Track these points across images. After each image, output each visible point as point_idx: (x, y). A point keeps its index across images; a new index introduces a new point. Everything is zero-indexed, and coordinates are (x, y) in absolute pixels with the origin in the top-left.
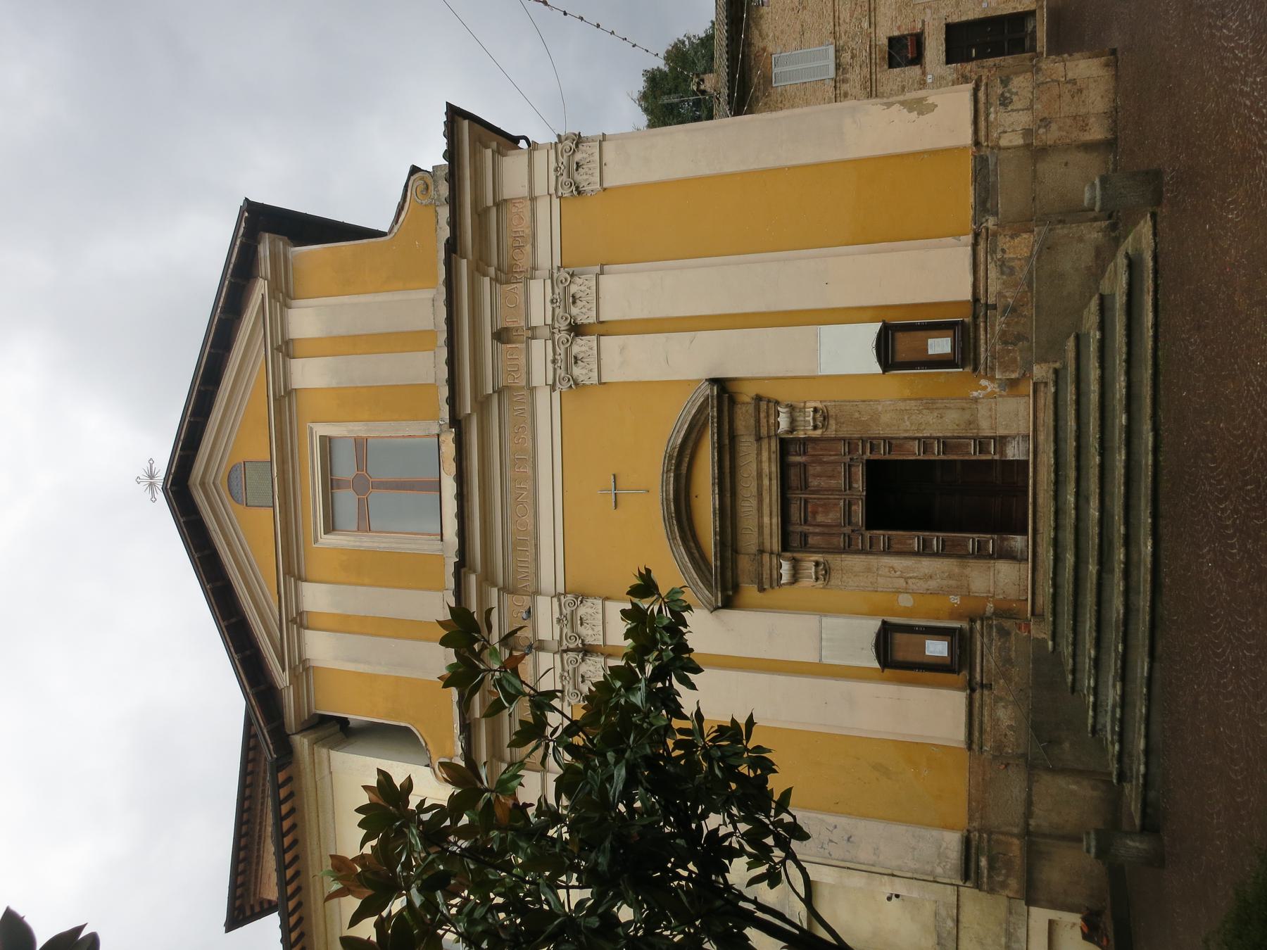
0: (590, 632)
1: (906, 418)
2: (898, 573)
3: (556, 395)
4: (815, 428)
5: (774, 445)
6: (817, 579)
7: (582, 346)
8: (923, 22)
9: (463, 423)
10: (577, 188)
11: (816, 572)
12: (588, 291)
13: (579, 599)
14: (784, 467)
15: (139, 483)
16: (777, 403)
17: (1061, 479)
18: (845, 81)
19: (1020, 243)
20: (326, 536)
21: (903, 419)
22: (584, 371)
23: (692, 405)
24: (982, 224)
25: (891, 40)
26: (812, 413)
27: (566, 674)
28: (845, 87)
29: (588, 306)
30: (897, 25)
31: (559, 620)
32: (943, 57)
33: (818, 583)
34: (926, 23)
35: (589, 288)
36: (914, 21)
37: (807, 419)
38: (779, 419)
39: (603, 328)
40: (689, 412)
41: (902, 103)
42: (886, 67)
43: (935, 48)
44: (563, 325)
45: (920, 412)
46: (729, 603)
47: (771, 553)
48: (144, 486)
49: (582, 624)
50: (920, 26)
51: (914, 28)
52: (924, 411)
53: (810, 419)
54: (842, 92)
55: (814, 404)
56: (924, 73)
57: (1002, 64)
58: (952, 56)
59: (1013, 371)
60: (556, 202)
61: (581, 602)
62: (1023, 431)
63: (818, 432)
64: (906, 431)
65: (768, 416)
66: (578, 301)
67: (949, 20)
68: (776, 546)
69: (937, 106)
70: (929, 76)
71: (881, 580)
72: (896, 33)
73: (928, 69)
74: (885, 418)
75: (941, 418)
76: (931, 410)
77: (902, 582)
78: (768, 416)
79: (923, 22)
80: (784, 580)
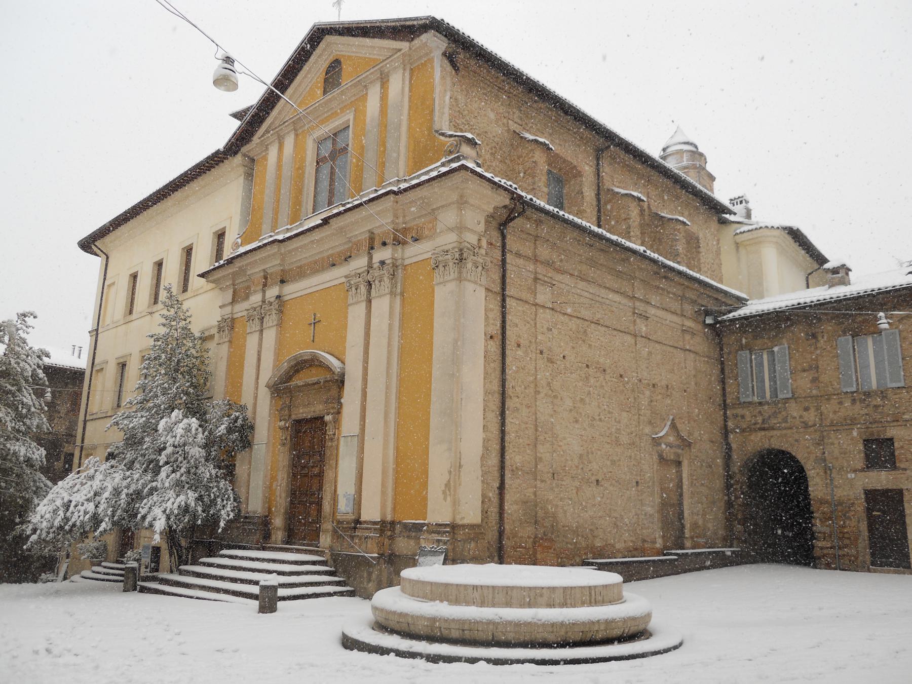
7: (363, 289)
8: (906, 470)
18: (854, 401)
25: (891, 440)
28: (847, 404)
30: (905, 445)
32: (870, 487)
34: (904, 472)
36: (907, 461)
42: (864, 437)
43: (881, 479)
50: (902, 466)
51: (900, 461)
54: (843, 400)
56: (855, 471)
57: (861, 538)
58: (872, 496)
67: (906, 493)
70: (853, 476)
72: (896, 444)
73: (860, 474)
79: (906, 470)
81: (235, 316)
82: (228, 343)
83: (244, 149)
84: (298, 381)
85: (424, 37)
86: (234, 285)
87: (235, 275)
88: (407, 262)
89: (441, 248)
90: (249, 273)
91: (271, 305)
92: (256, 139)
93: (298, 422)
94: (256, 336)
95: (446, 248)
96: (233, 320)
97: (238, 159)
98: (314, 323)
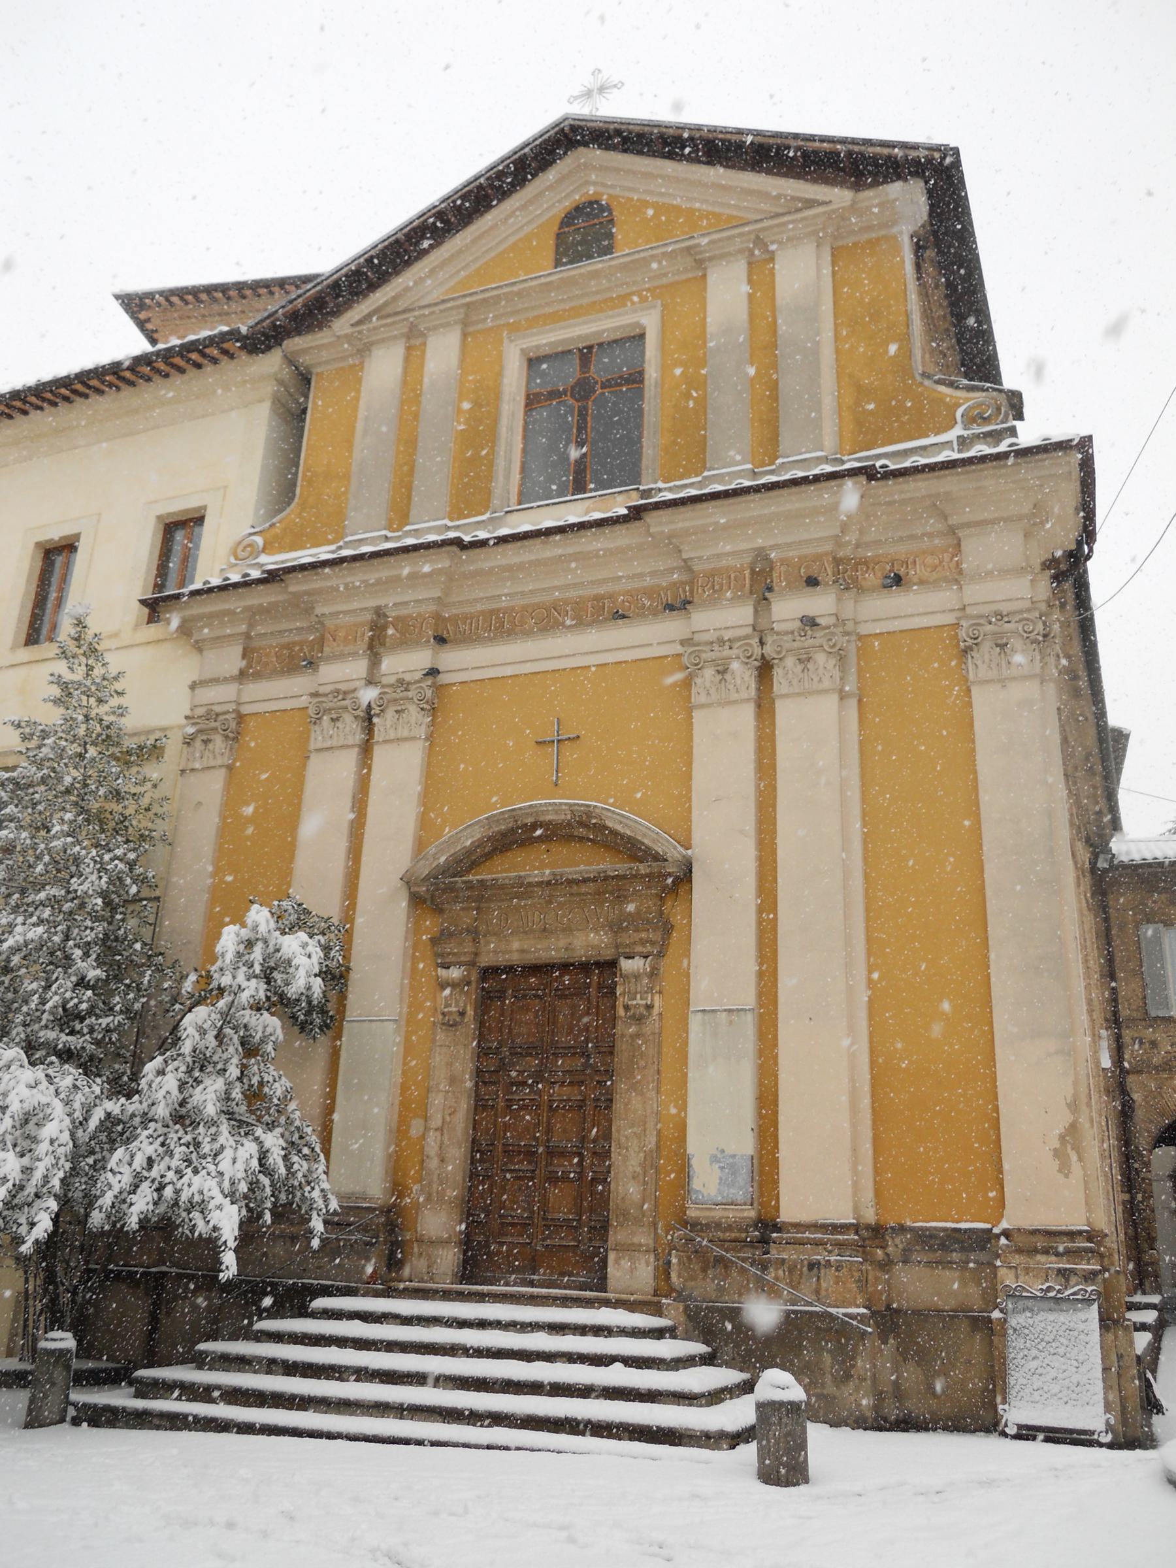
0: (389, 723)
1: (635, 1129)
2: (448, 1119)
3: (678, 649)
4: (627, 1008)
5: (608, 955)
6: (444, 1014)
7: (743, 676)
9: (637, 523)
10: (970, 648)
11: (450, 1013)
12: (816, 679)
13: (425, 706)
14: (585, 967)
15: (593, 74)
16: (661, 955)
17: (1064, 1306)
19: (850, 1291)
20: (518, 352)
21: (633, 1126)
22: (708, 684)
23: (654, 841)
24: (893, 1238)
26: (644, 1002)
27: (340, 697)
29: (795, 682)
31: (401, 682)
33: (441, 1017)
35: (820, 681)
37: (638, 996)
38: (637, 958)
39: (764, 707)
40: (644, 835)
41: (1073, 1128)
44: (769, 650)
45: (641, 1149)
46: (416, 900)
47: (476, 954)
48: (588, 81)
49: (397, 712)
52: (642, 1155)
53: (638, 1001)
55: (657, 1005)
59: (679, 1276)
60: (949, 619)
61: (422, 709)
62: (611, 1283)
63: (621, 1012)
64: (618, 1131)
65: (643, 942)
66: (803, 666)
68: (485, 961)
69: (1067, 1176)
71: (441, 1097)
74: (636, 1101)
75: (634, 1178)
76: (643, 1165)
77: (436, 1122)
78: (643, 942)
80: (442, 972)
81: (245, 710)
82: (223, 770)
83: (296, 343)
84: (502, 871)
85: (895, 189)
86: (247, 636)
87: (254, 614)
88: (864, 629)
89: (994, 607)
90: (319, 610)
91: (407, 690)
92: (342, 325)
93: (489, 972)
94: (348, 761)
95: (1005, 608)
96: (241, 718)
97: (271, 363)
98: (559, 741)
